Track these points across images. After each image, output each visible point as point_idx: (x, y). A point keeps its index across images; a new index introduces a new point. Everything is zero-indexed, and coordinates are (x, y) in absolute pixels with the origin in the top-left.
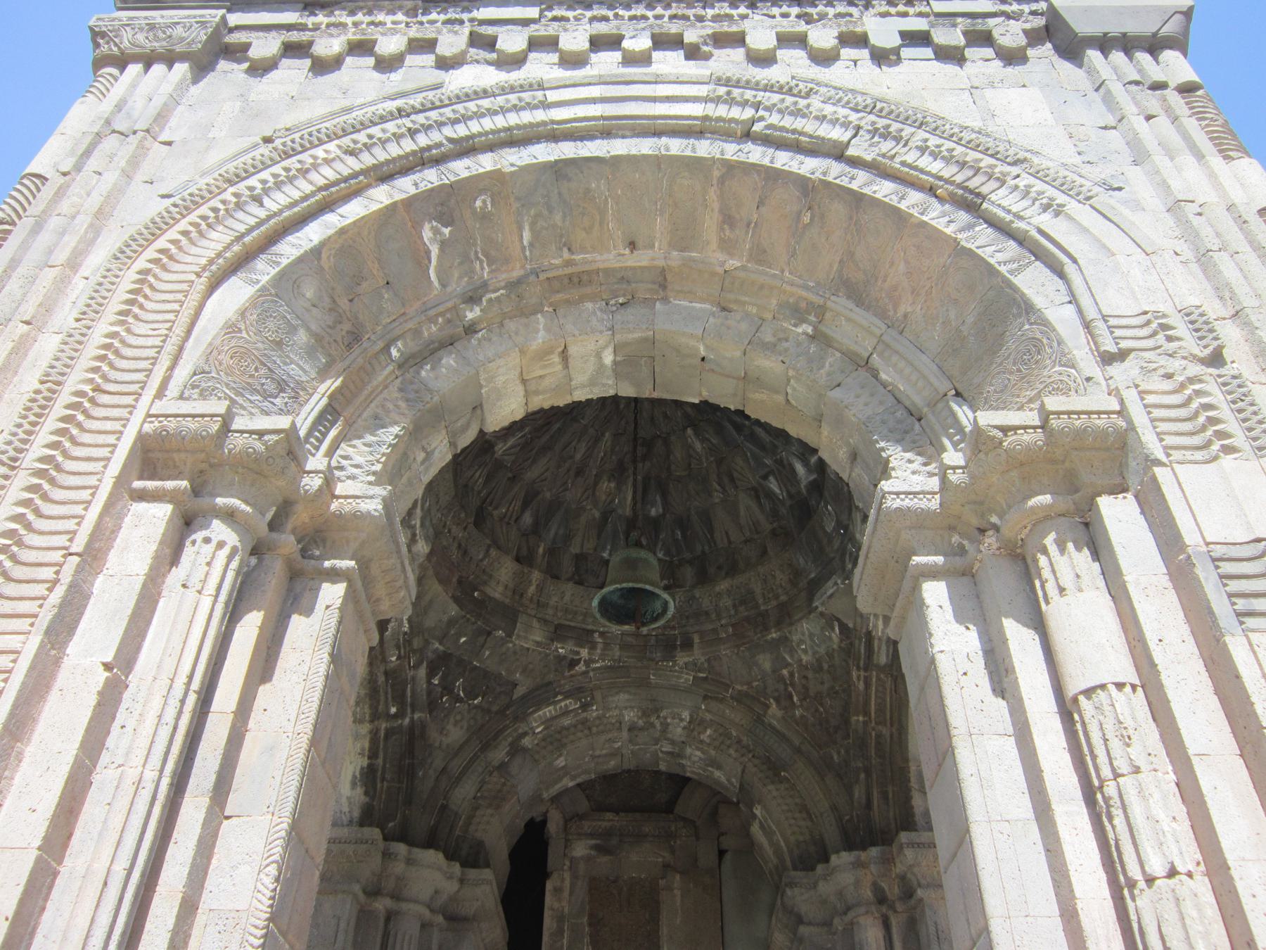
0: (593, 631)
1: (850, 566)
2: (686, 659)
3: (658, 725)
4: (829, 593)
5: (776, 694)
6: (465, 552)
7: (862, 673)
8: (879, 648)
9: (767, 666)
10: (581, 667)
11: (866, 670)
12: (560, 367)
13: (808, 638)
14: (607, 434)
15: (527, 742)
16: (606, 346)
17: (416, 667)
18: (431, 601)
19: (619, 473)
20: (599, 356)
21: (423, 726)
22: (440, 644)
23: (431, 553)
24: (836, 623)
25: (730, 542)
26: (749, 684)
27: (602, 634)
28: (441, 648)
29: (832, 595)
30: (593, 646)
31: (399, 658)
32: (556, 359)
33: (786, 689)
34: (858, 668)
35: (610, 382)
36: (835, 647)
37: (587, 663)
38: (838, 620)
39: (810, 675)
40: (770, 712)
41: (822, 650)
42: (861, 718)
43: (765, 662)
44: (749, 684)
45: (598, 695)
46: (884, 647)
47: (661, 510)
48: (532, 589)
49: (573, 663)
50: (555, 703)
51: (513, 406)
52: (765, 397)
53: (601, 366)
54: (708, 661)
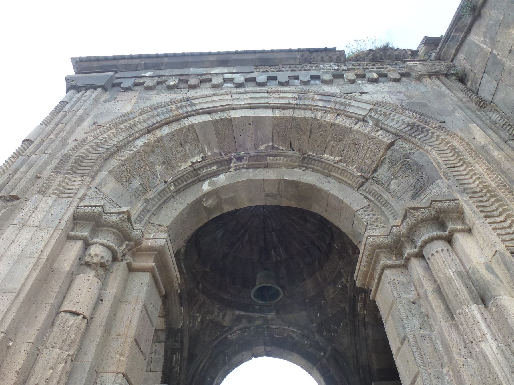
10: (348, 285)
22: (313, 323)
23: (278, 313)
50: (358, 301)
51: (159, 321)
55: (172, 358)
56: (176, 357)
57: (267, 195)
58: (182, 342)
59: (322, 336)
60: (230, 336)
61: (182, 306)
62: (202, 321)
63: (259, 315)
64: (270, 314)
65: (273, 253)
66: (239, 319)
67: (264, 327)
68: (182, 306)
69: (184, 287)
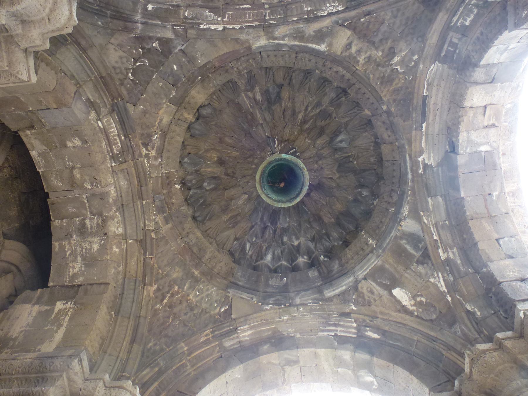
0: (161, 157)
1: (271, 302)
2: (160, 223)
3: (111, 213)
4: (241, 296)
5: (161, 288)
6: (227, 71)
7: (211, 335)
8: (232, 339)
9: (175, 275)
10: (144, 151)
11: (213, 337)
12: (486, 124)
13: (206, 295)
14: (238, 153)
15: (93, 114)
16: (491, 146)
17: (175, 31)
18: (215, 46)
19: (221, 162)
20: (487, 143)
21: (127, 30)
22: (181, 50)
23: (249, 48)
24: (227, 307)
25: (206, 231)
26: (159, 268)
27: (160, 164)
28: (177, 50)
29: (243, 298)
30: (156, 158)
31: (186, 18)
32: (491, 122)
33: (168, 292)
34: (212, 332)
35: (468, 151)
36: (212, 312)
37: (147, 156)
38: (231, 307)
39: (185, 304)
40: (149, 288)
41: (204, 306)
42: (186, 348)
43: (177, 274)
44: (159, 268)
45: (124, 166)
46: (235, 341)
47: (208, 188)
48: (186, 115)
49: (146, 145)
50: (119, 135)
51: (475, 100)
52: (488, 228)
53: (480, 145)
54: (164, 237)
55: (472, 21)
56: (466, 20)
57: (297, 362)
58: (443, 38)
59: (159, 39)
60: (340, 8)
61: (425, 98)
62: (392, 53)
63: (282, 42)
64: (264, 45)
65: (259, 97)
66: (320, 36)
67: (271, 22)
68: (425, 98)
69: (414, 132)
